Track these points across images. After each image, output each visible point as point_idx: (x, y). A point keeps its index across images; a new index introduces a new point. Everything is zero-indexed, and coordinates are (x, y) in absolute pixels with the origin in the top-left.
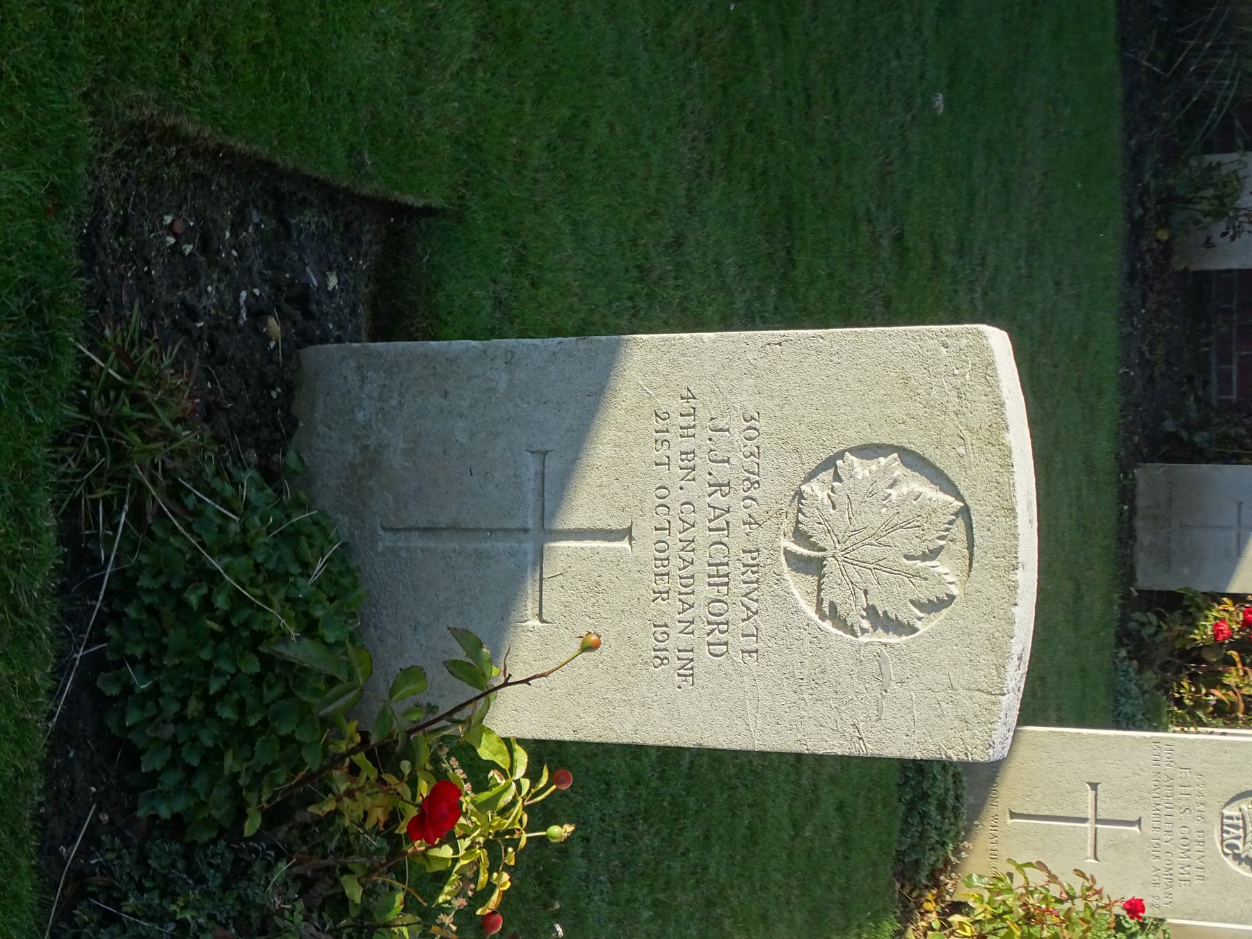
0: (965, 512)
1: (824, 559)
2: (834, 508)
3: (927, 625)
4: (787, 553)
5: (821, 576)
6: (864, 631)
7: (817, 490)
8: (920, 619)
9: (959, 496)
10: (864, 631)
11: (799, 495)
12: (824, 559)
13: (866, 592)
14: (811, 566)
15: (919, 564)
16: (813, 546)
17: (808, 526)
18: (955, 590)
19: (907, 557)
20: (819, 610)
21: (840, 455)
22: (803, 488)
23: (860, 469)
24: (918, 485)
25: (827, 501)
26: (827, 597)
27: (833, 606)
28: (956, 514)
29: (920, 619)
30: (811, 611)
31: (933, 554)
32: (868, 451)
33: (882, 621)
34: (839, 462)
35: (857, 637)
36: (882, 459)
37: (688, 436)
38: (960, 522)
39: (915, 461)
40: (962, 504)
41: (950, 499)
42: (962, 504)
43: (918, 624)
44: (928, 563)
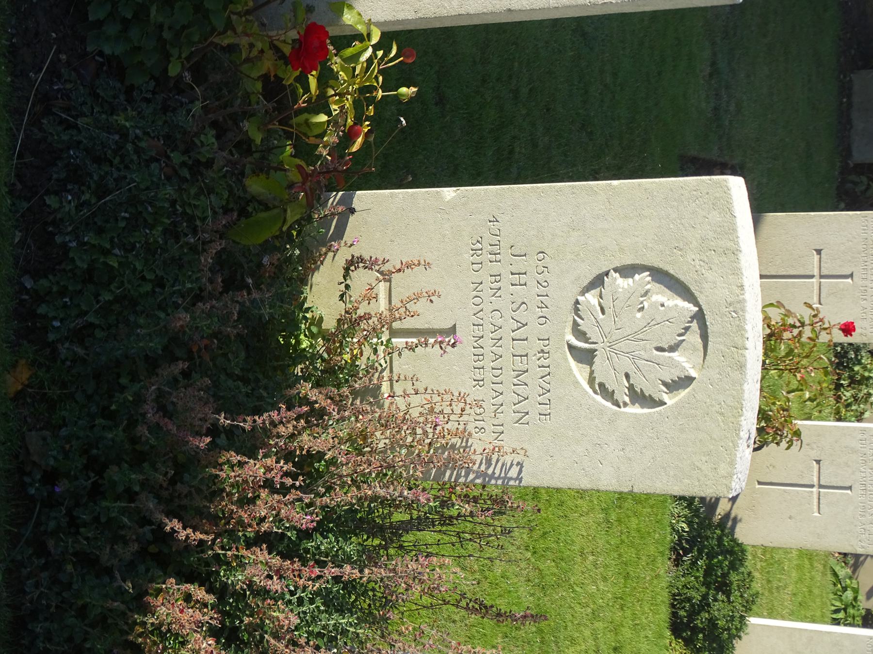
0: (700, 317)
1: (596, 350)
2: (603, 311)
4: (571, 347)
9: (696, 303)
10: (625, 404)
11: (577, 302)
12: (596, 350)
13: (627, 376)
14: (586, 357)
15: (666, 354)
17: (583, 326)
18: (693, 373)
19: (660, 349)
22: (581, 298)
23: (622, 283)
24: (662, 296)
25: (598, 308)
27: (601, 385)
28: (693, 318)
32: (627, 271)
33: (639, 397)
34: (605, 278)
35: (619, 406)
36: (637, 277)
37: (496, 261)
38: (694, 325)
40: (697, 309)
42: (697, 309)
43: (666, 398)
44: (671, 354)
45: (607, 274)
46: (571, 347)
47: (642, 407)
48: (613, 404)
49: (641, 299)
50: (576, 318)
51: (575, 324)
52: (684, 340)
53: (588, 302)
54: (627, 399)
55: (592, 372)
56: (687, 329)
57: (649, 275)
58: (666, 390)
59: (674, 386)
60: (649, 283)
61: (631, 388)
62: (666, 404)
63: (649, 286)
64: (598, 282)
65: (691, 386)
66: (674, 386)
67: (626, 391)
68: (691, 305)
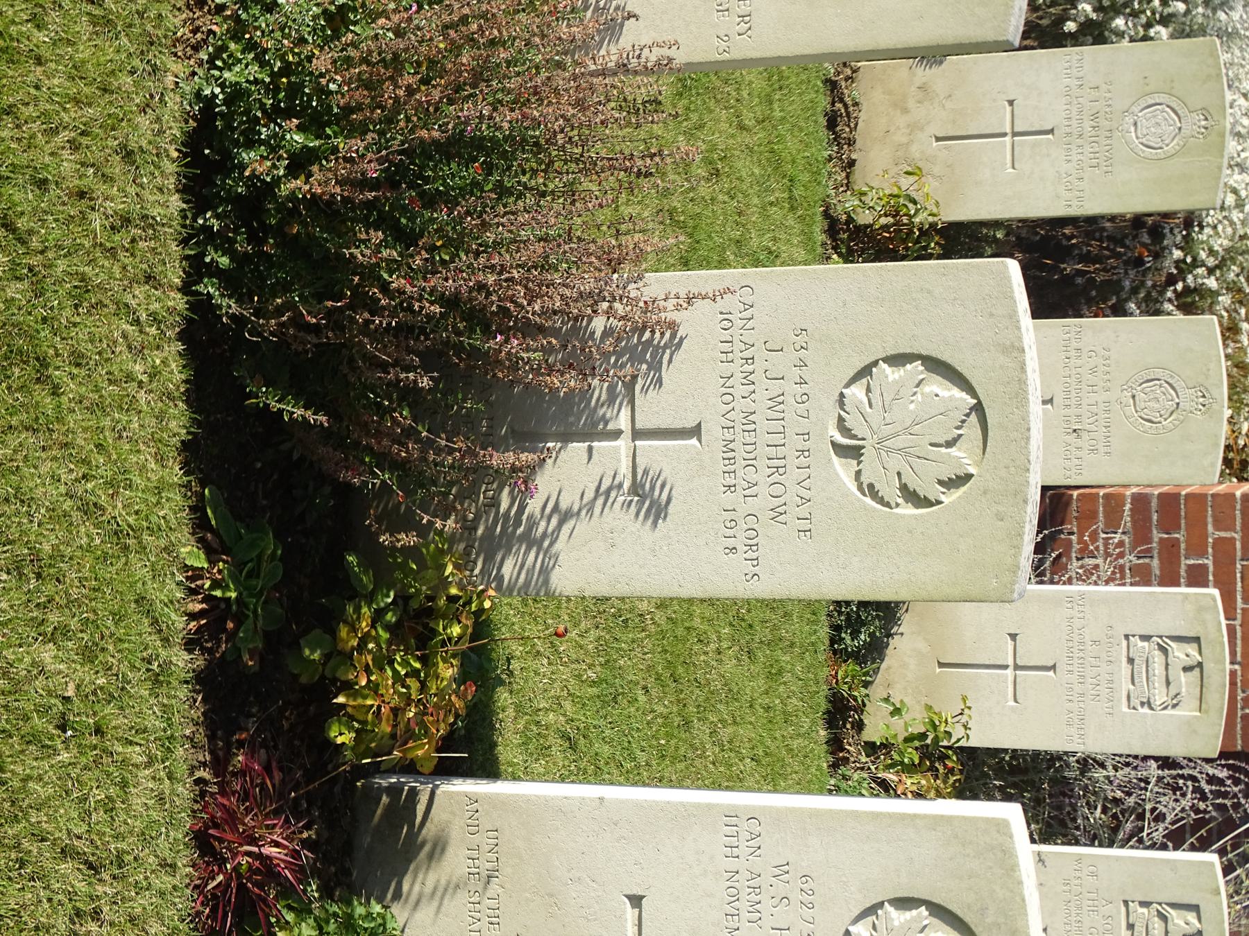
0: (979, 409)
1: (864, 447)
2: (871, 406)
3: (951, 498)
4: (834, 444)
5: (859, 463)
6: (897, 505)
7: (857, 392)
8: (943, 493)
10: (897, 505)
11: (842, 395)
12: (864, 447)
13: (899, 474)
15: (943, 450)
16: (854, 437)
18: (972, 470)
19: (932, 445)
20: (860, 488)
21: (875, 363)
25: (865, 400)
26: (866, 480)
27: (871, 486)
28: (971, 409)
29: (943, 493)
30: (853, 487)
31: (950, 444)
34: (874, 369)
35: (891, 508)
36: (908, 367)
38: (973, 418)
39: (937, 366)
40: (975, 401)
41: (964, 395)
42: (975, 401)
43: (943, 498)
44: (949, 450)
45: (875, 363)
46: (834, 444)
47: (917, 508)
48: (883, 505)
49: (915, 390)
50: (842, 413)
51: (841, 420)
52: (961, 435)
53: (854, 394)
54: (900, 501)
55: (858, 473)
56: (963, 422)
57: (922, 365)
58: (944, 490)
59: (950, 483)
60: (922, 372)
61: (904, 488)
62: (941, 502)
63: (921, 377)
64: (865, 371)
65: (968, 485)
66: (950, 483)
67: (898, 491)
68: (969, 397)
